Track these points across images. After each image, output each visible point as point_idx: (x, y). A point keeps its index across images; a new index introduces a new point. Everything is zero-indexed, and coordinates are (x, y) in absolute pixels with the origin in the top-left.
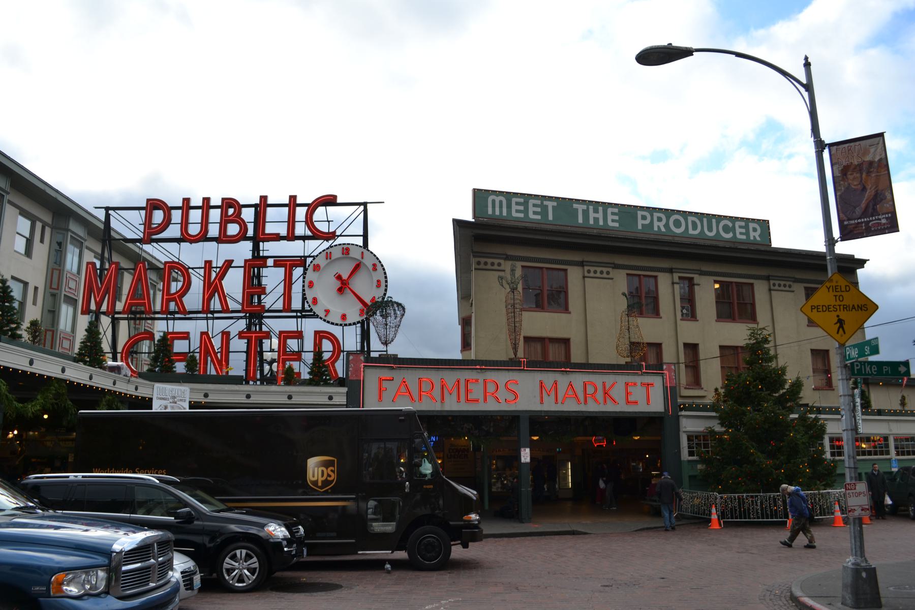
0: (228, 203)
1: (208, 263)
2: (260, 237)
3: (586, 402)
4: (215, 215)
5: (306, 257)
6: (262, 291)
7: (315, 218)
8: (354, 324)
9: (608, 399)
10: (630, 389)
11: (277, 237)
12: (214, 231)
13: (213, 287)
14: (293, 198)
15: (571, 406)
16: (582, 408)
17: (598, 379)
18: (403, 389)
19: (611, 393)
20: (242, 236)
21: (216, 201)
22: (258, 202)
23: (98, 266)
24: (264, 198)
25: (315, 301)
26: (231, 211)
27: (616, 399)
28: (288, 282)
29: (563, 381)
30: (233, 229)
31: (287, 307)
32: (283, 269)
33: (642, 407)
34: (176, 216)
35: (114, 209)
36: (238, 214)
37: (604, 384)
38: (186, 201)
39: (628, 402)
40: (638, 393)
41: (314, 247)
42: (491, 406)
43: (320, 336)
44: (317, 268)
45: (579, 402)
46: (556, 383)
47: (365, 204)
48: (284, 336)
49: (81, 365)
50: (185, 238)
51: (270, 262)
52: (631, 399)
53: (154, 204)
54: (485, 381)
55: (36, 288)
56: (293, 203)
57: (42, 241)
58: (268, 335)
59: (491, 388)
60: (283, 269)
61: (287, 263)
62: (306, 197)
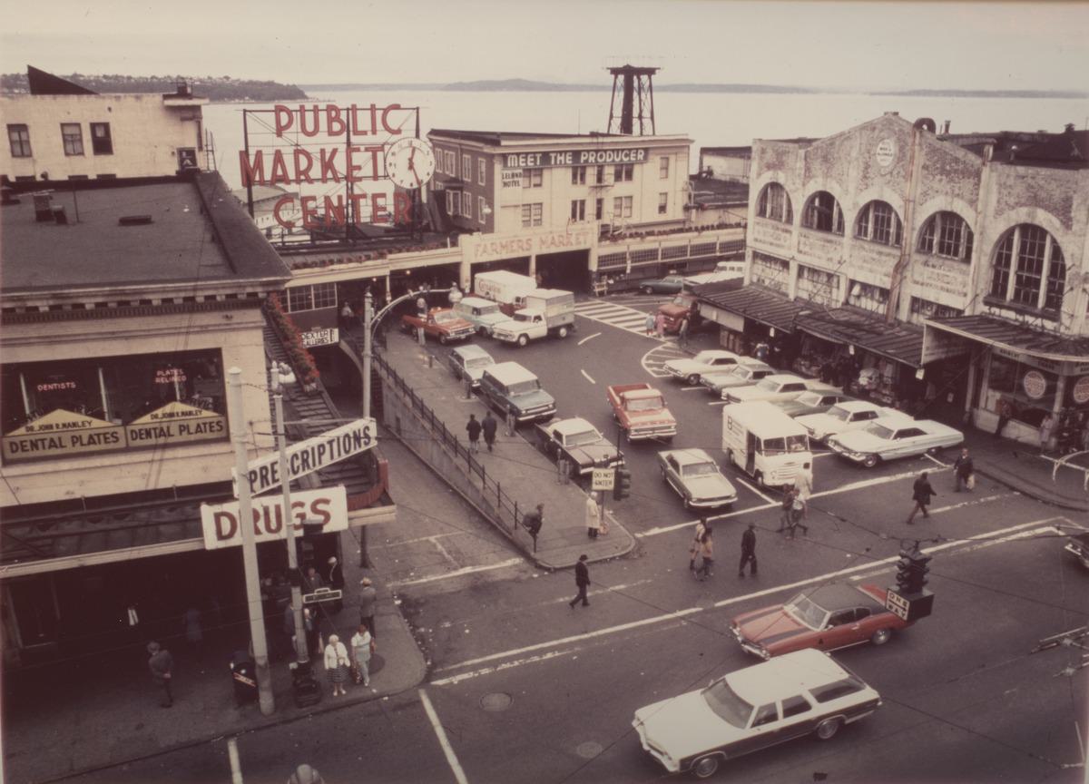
0: (330, 108)
1: (323, 151)
2: (349, 129)
4: (323, 116)
5: (383, 145)
11: (365, 133)
13: (327, 165)
21: (322, 106)
22: (350, 107)
25: (394, 175)
26: (333, 114)
28: (375, 159)
30: (336, 127)
32: (370, 153)
34: (297, 116)
35: (250, 111)
44: (393, 154)
47: (418, 109)
48: (375, 197)
51: (362, 148)
56: (373, 109)
58: (364, 196)
60: (370, 153)
61: (374, 150)
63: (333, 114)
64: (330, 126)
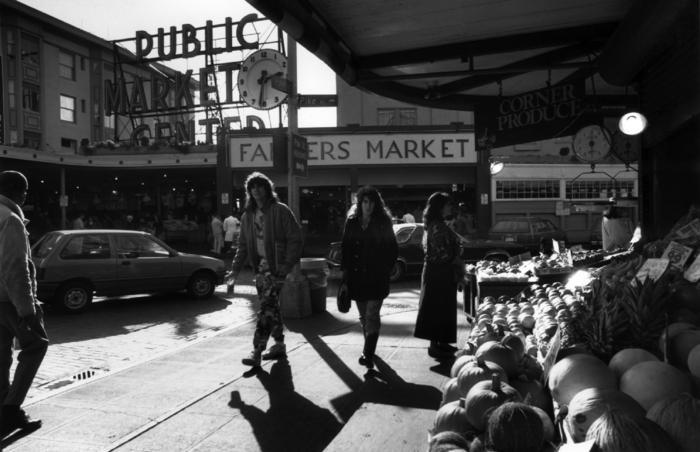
0: (187, 28)
2: (211, 51)
3: (407, 156)
4: (179, 38)
6: (215, 89)
7: (244, 33)
8: (272, 108)
9: (427, 155)
10: (447, 145)
11: (220, 51)
12: (179, 50)
14: (229, 20)
15: (394, 160)
16: (404, 161)
17: (418, 138)
18: (259, 152)
19: (429, 149)
20: (197, 52)
21: (179, 28)
23: (113, 82)
24: (209, 23)
26: (189, 34)
27: (434, 153)
29: (387, 140)
30: (191, 47)
31: (229, 100)
33: (457, 159)
34: (155, 41)
36: (194, 34)
37: (423, 142)
38: (161, 31)
39: (444, 156)
40: (454, 148)
41: (247, 53)
42: (328, 161)
43: (250, 119)
45: (400, 156)
46: (381, 142)
49: (26, 149)
50: (163, 57)
51: (217, 68)
52: (447, 152)
53: (141, 35)
54: (323, 144)
55: (83, 102)
56: (229, 23)
57: (83, 68)
59: (327, 148)
61: (228, 68)
62: (236, 18)
63: (189, 34)
64: (185, 48)
